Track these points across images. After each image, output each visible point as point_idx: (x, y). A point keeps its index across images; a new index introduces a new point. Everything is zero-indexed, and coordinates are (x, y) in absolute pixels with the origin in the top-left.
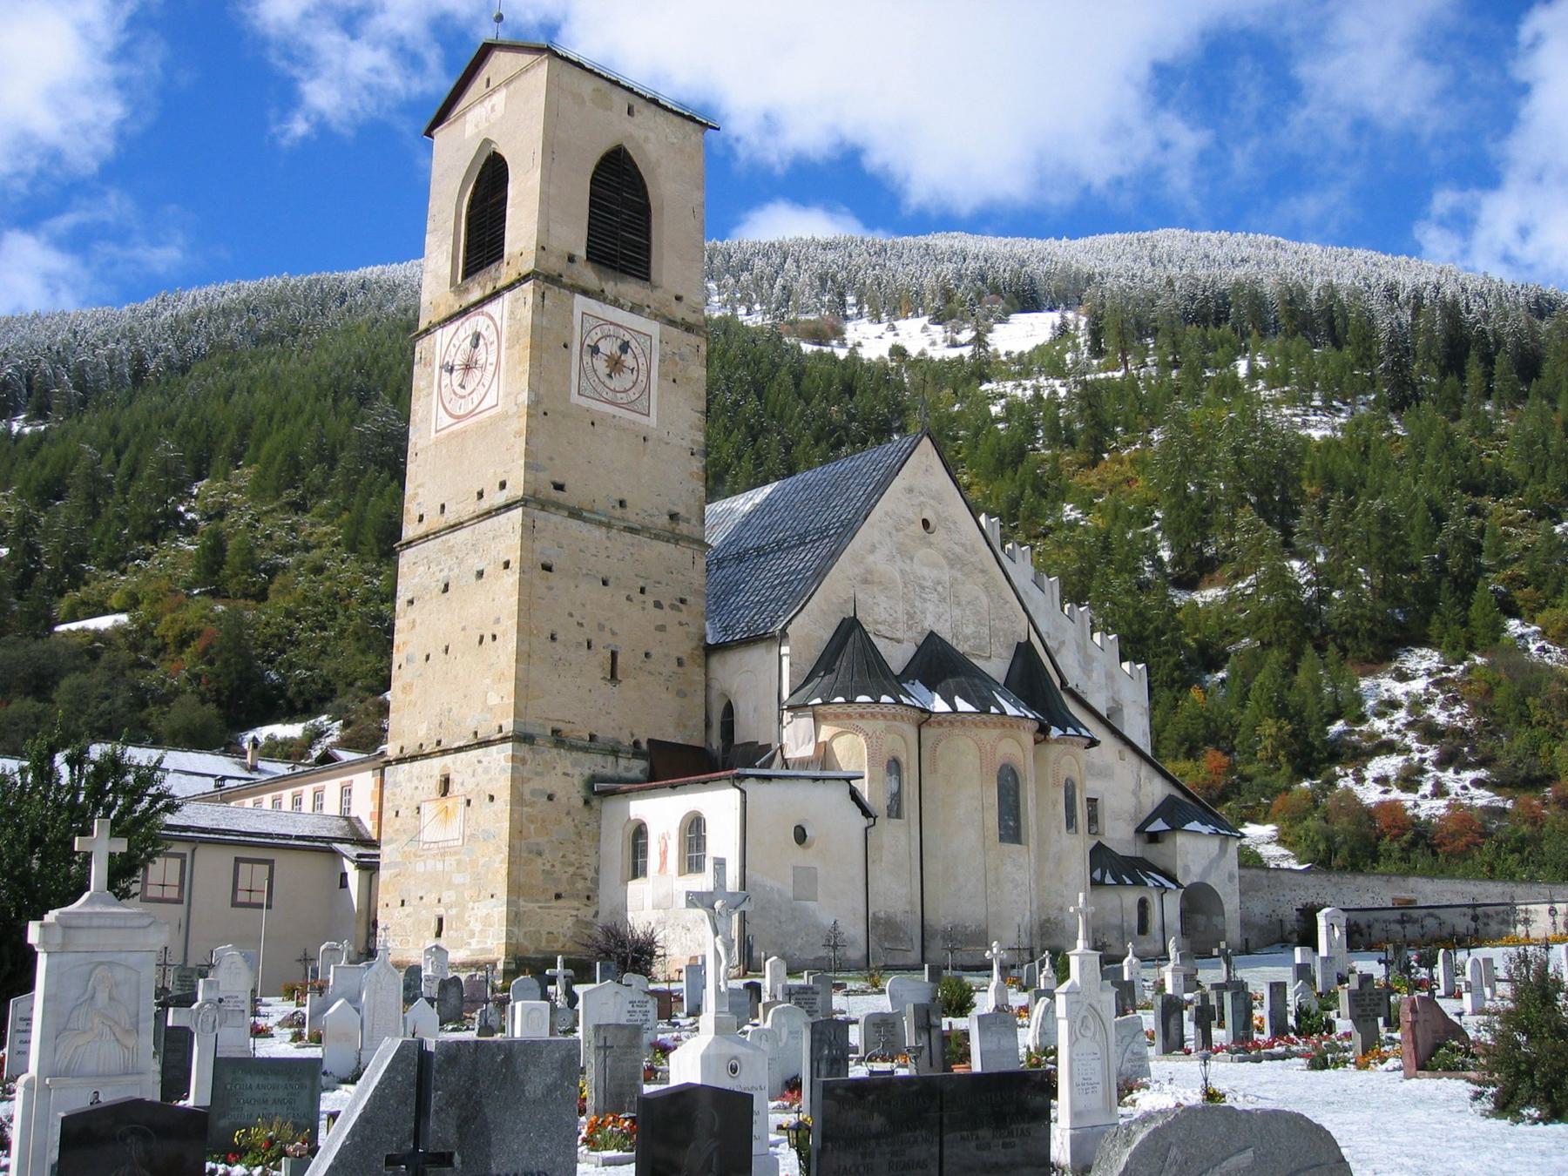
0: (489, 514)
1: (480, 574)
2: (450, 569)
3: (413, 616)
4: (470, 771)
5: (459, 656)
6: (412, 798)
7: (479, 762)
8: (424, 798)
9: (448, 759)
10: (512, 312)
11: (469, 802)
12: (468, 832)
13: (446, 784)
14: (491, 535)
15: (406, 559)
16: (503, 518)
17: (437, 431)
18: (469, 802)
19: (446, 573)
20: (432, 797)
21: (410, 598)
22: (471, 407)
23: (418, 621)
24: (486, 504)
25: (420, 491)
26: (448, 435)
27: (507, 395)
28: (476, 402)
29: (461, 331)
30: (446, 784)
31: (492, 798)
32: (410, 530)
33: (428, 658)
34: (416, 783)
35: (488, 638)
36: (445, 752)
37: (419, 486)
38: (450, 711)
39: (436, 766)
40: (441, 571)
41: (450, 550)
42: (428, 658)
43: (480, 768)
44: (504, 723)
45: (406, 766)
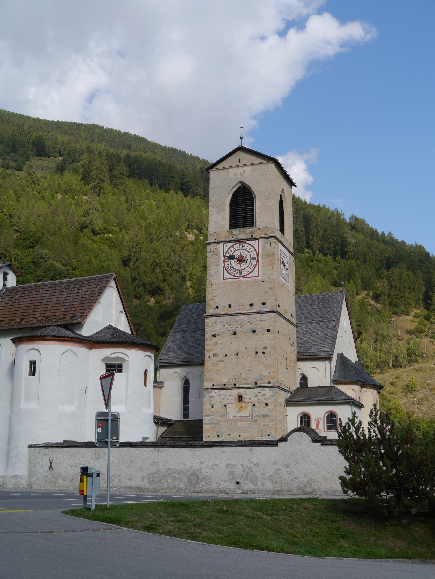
0: (259, 313)
1: (254, 332)
2: (236, 328)
3: (216, 341)
4: (254, 395)
5: (244, 357)
6: (221, 402)
7: (259, 392)
8: (229, 402)
9: (242, 391)
10: (264, 247)
11: (254, 405)
12: (254, 415)
13: (240, 398)
14: (259, 319)
15: (209, 321)
16: (266, 315)
17: (223, 279)
18: (254, 405)
19: (234, 328)
20: (233, 402)
21: (214, 334)
22: (243, 275)
23: (219, 343)
24: (256, 308)
25: (215, 298)
26: (231, 281)
27: (263, 274)
28: (246, 273)
29: (235, 246)
30: (240, 398)
31: (267, 404)
32: (210, 311)
33: (226, 355)
34: (223, 397)
35: (260, 353)
36: (239, 388)
37: (214, 296)
38: (241, 374)
39: (235, 393)
40: (231, 328)
41: (237, 321)
42: (226, 355)
43: (259, 395)
44: (271, 381)
45: (217, 391)
